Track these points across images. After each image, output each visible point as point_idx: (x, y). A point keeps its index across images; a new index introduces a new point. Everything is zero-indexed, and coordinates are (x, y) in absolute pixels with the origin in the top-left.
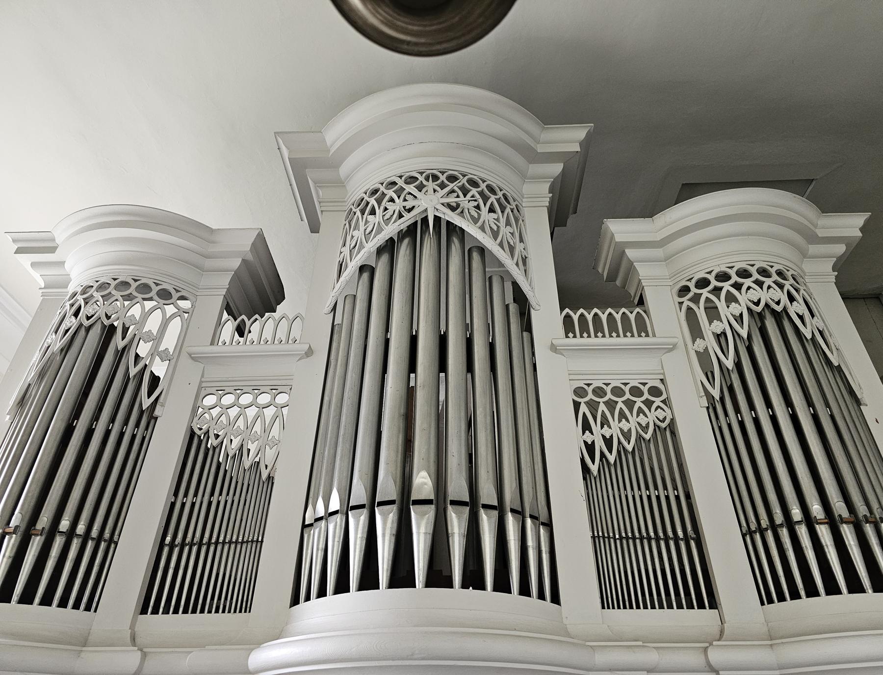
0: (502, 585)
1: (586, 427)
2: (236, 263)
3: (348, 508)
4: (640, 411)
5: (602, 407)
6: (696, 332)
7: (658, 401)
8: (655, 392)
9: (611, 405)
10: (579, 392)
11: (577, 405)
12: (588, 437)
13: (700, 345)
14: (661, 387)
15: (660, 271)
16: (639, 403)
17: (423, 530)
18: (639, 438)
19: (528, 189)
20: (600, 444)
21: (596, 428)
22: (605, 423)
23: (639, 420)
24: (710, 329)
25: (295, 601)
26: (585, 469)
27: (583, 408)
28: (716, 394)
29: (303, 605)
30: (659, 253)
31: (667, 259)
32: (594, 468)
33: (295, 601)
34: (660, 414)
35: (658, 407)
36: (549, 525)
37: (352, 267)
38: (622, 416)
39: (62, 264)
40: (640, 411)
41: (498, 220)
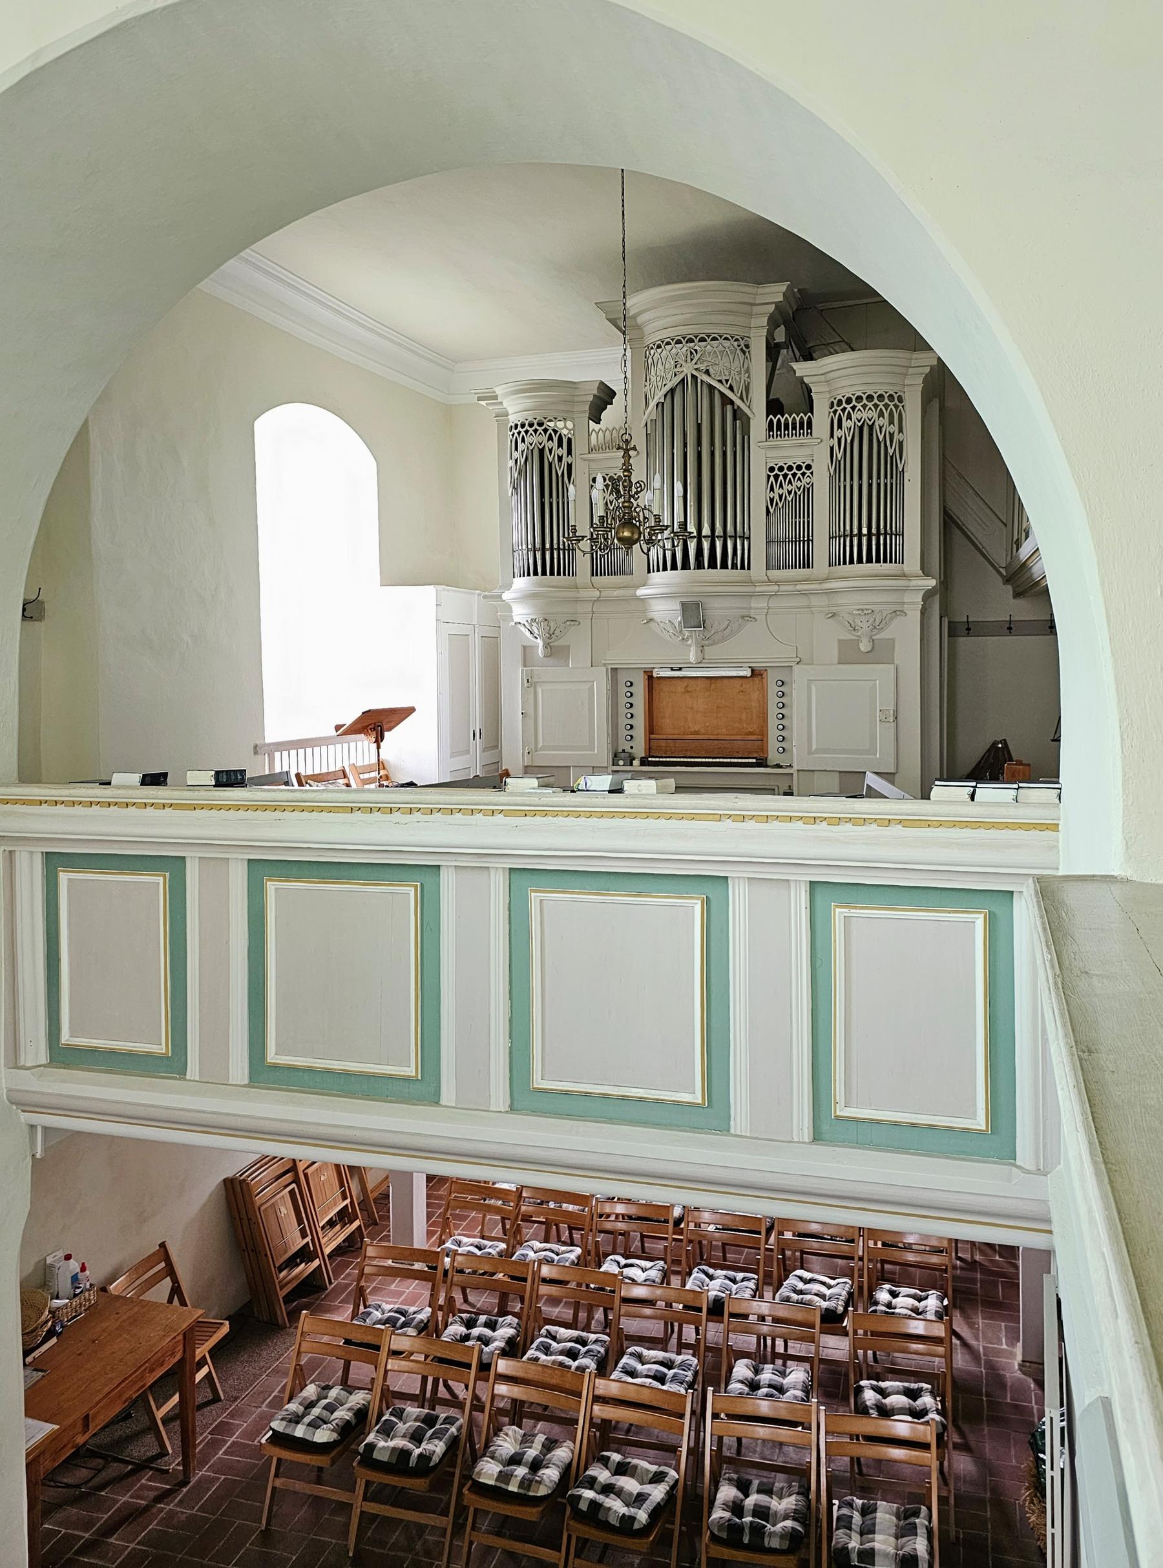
2: (591, 398)
4: (799, 479)
5: (781, 478)
6: (832, 436)
7: (808, 473)
8: (809, 467)
9: (785, 476)
11: (769, 477)
12: (772, 495)
14: (811, 464)
18: (795, 493)
20: (777, 498)
22: (781, 486)
24: (838, 433)
25: (649, 572)
26: (768, 512)
27: (772, 479)
29: (652, 574)
30: (823, 378)
32: (772, 510)
33: (649, 572)
34: (808, 480)
35: (808, 476)
36: (749, 538)
37: (652, 404)
38: (790, 482)
40: (799, 479)
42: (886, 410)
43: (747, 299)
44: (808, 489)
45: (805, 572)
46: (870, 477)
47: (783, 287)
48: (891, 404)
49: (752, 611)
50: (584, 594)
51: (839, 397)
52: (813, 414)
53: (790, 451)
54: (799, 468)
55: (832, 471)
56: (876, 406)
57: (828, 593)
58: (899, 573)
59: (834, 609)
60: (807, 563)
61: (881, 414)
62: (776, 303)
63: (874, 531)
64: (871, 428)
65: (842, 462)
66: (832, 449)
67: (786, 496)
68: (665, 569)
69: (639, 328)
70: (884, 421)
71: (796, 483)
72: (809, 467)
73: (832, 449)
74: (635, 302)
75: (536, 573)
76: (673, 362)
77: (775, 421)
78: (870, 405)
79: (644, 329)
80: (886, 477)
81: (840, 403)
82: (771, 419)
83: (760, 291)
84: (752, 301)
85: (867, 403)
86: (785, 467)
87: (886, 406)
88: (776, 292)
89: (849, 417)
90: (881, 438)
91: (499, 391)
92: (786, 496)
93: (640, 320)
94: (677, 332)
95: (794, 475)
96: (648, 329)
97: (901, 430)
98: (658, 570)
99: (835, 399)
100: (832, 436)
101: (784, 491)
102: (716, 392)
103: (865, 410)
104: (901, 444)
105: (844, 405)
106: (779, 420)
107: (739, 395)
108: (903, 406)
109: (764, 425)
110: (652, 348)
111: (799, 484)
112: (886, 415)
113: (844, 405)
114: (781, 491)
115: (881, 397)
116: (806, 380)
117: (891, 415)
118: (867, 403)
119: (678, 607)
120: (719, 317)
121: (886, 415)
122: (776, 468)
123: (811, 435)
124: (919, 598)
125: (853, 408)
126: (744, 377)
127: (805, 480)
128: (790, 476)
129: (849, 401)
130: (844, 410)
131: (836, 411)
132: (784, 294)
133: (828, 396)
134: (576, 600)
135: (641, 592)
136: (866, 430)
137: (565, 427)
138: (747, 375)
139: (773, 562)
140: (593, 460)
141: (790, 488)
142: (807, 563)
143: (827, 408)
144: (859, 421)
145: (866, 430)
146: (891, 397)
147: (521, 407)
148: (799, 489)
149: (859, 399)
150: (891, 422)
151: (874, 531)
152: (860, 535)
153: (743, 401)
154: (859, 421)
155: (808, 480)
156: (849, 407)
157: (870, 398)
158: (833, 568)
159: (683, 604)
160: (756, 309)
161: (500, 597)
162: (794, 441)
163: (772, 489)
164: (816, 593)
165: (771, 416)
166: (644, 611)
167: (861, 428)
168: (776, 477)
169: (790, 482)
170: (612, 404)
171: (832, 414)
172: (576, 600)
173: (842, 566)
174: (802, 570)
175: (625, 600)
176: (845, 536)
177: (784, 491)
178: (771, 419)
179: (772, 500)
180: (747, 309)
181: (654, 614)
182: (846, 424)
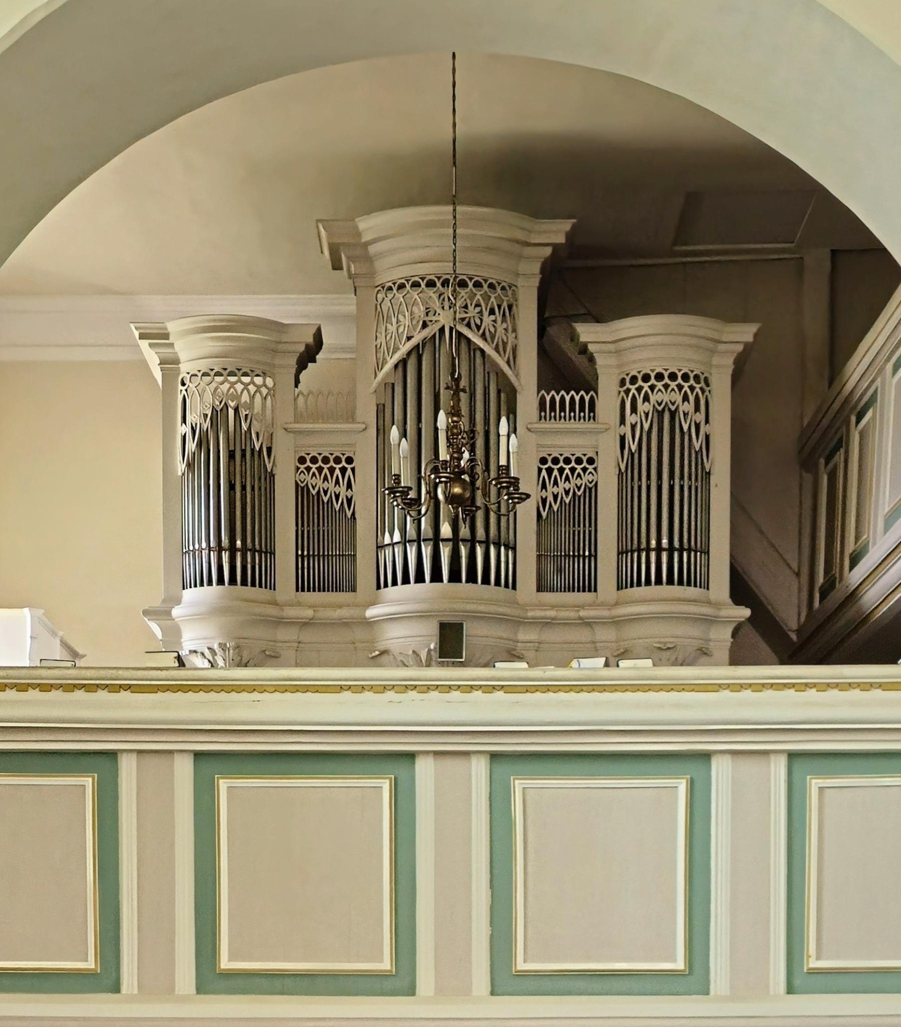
0: (486, 581)
1: (544, 486)
3: (404, 542)
4: (579, 475)
5: (556, 473)
6: (623, 421)
7: (590, 468)
8: (591, 461)
9: (561, 470)
10: (543, 461)
11: (540, 470)
12: (544, 494)
14: (595, 458)
15: (612, 361)
16: (579, 468)
17: (446, 554)
18: (574, 493)
20: (550, 499)
22: (556, 483)
23: (576, 482)
27: (544, 473)
28: (623, 469)
30: (612, 347)
31: (617, 352)
32: (544, 514)
33: (379, 587)
34: (590, 478)
36: (514, 549)
38: (567, 478)
39: (171, 345)
40: (579, 475)
41: (495, 321)
42: (692, 394)
44: (590, 489)
45: (586, 597)
47: (566, 225)
48: (698, 386)
49: (519, 644)
50: (291, 612)
51: (634, 373)
52: (597, 394)
54: (579, 461)
55: (623, 469)
56: (680, 387)
57: (617, 622)
59: (624, 645)
60: (590, 586)
61: (685, 398)
63: (676, 544)
64: (673, 414)
65: (636, 456)
66: (623, 439)
67: (562, 498)
68: (406, 581)
69: (369, 259)
70: (689, 407)
71: (574, 481)
72: (591, 461)
73: (623, 439)
75: (221, 581)
76: (422, 308)
77: (548, 398)
78: (673, 385)
81: (634, 380)
82: (543, 395)
85: (669, 382)
86: (561, 459)
87: (692, 388)
89: (646, 399)
91: (172, 327)
92: (562, 498)
93: (372, 249)
94: (428, 270)
96: (379, 265)
97: (707, 421)
98: (395, 583)
99: (627, 375)
100: (623, 421)
101: (560, 490)
102: (478, 354)
103: (666, 391)
104: (707, 437)
105: (640, 383)
107: (506, 359)
108: (709, 391)
111: (579, 482)
112: (692, 398)
114: (555, 490)
115: (686, 377)
116: (591, 348)
117: (697, 399)
118: (669, 382)
121: (692, 398)
122: (550, 459)
123: (594, 420)
125: (652, 388)
126: (511, 336)
127: (587, 478)
128: (567, 471)
129: (646, 378)
130: (639, 389)
133: (617, 371)
135: (370, 612)
137: (265, 385)
138: (514, 335)
140: (300, 432)
141: (567, 486)
142: (590, 586)
143: (615, 386)
144: (660, 404)
146: (697, 378)
147: (195, 354)
148: (579, 488)
149: (660, 377)
153: (511, 368)
154: (660, 404)
155: (590, 478)
156: (646, 386)
157: (673, 376)
158: (621, 592)
161: (168, 613)
162: (573, 425)
163: (544, 486)
165: (543, 392)
166: (373, 641)
167: (661, 414)
168: (550, 471)
169: (567, 478)
170: (314, 361)
171: (622, 394)
173: (635, 589)
174: (581, 594)
175: (345, 624)
177: (560, 490)
178: (543, 395)
179: (544, 501)
182: (642, 407)
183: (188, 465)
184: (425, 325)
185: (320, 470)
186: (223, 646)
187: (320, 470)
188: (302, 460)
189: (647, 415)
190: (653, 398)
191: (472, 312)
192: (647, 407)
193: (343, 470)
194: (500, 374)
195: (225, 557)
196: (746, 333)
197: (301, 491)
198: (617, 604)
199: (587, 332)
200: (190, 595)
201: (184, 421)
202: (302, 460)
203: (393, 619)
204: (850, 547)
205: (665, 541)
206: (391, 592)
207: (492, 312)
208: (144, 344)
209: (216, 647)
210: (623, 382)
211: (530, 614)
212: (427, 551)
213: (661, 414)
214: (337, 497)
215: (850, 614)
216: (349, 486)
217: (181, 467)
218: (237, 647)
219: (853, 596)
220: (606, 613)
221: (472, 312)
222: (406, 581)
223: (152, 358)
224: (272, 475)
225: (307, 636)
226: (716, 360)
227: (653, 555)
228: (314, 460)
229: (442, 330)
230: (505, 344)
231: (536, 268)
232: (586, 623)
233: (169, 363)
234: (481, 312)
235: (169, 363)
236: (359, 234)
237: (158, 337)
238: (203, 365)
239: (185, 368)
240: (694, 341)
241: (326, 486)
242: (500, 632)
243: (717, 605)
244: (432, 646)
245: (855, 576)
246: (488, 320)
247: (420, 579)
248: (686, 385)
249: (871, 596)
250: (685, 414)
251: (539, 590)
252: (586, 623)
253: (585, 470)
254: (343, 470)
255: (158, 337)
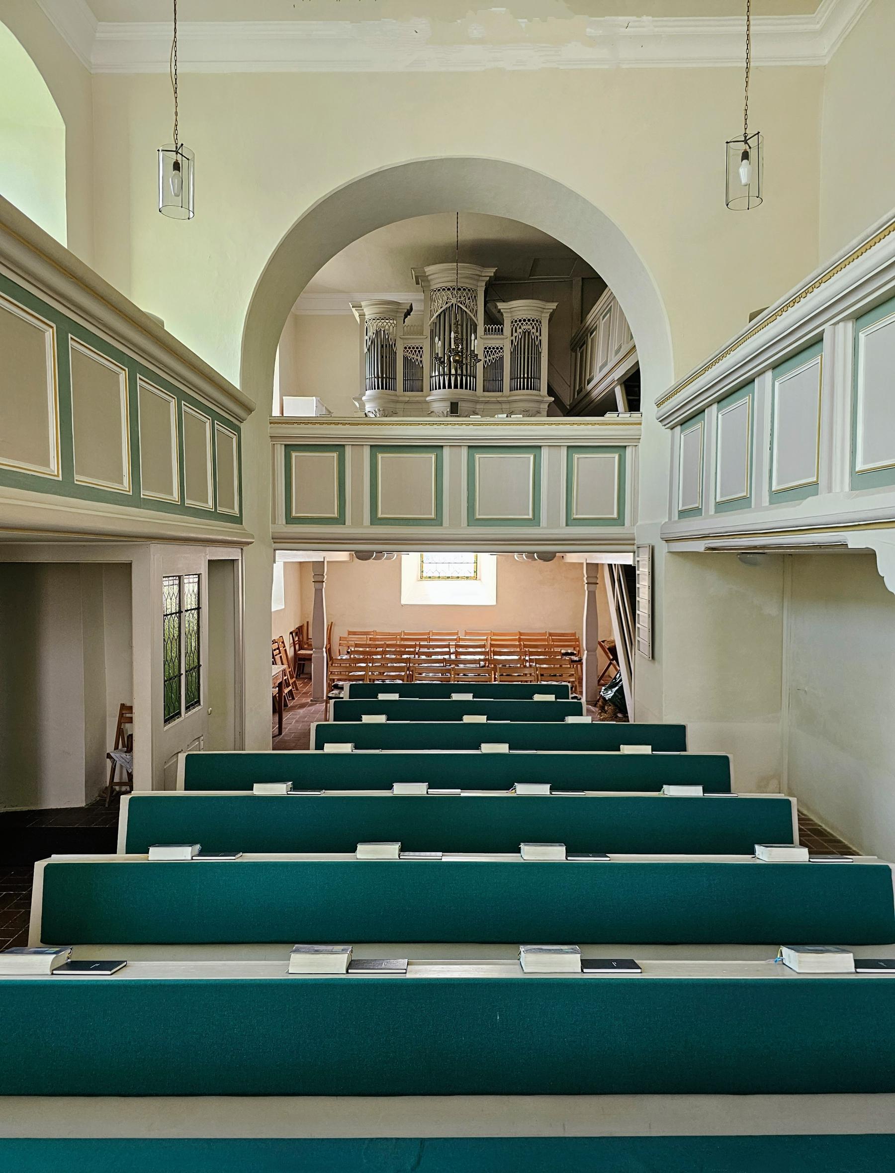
0: (466, 388)
1: (486, 357)
3: (439, 375)
6: (512, 335)
7: (501, 351)
8: (501, 348)
9: (492, 352)
10: (486, 348)
11: (484, 351)
12: (486, 359)
13: (512, 338)
15: (509, 315)
18: (496, 359)
19: (480, 284)
20: (488, 361)
21: (488, 357)
22: (490, 356)
24: (515, 334)
25: (431, 390)
26: (484, 366)
27: (486, 352)
28: (512, 351)
30: (509, 310)
32: (486, 366)
33: (431, 390)
34: (501, 354)
38: (494, 354)
39: (363, 310)
40: (497, 353)
41: (470, 302)
43: (478, 273)
45: (500, 394)
46: (528, 354)
48: (537, 324)
50: (401, 399)
53: (494, 341)
54: (497, 348)
55: (512, 351)
56: (532, 324)
57: (509, 402)
58: (539, 394)
59: (513, 409)
60: (501, 390)
61: (533, 328)
62: (490, 277)
63: (530, 376)
64: (529, 333)
66: (512, 341)
68: (440, 388)
69: (428, 281)
70: (534, 331)
72: (501, 348)
73: (512, 341)
74: (429, 270)
76: (446, 297)
78: (529, 323)
79: (431, 283)
80: (532, 354)
83: (485, 271)
84: (480, 274)
87: (535, 324)
88: (491, 272)
89: (520, 328)
90: (533, 337)
91: (363, 304)
93: (429, 278)
94: (449, 285)
95: (495, 351)
96: (432, 283)
97: (540, 335)
100: (512, 335)
104: (540, 340)
106: (495, 327)
109: (483, 329)
110: (435, 291)
112: (535, 328)
113: (518, 322)
114: (490, 358)
115: (533, 321)
116: (502, 310)
119: (449, 404)
120: (465, 279)
121: (535, 328)
124: (546, 406)
125: (522, 324)
129: (520, 321)
130: (518, 324)
131: (514, 325)
132: (494, 273)
133: (510, 318)
134: (397, 402)
136: (527, 333)
137: (393, 323)
139: (486, 389)
140: (406, 339)
142: (501, 390)
143: (510, 324)
145: (527, 333)
146: (537, 321)
147: (370, 312)
149: (524, 320)
150: (537, 331)
151: (530, 376)
152: (524, 378)
155: (501, 354)
157: (529, 320)
159: (451, 403)
160: (481, 278)
163: (486, 357)
164: (505, 402)
166: (429, 408)
168: (488, 352)
169: (494, 354)
170: (410, 315)
172: (397, 402)
176: (517, 378)
180: (476, 277)
181: (435, 410)
182: (519, 330)
183: (368, 349)
184: (447, 303)
185: (411, 351)
186: (379, 410)
187: (411, 351)
188: (406, 348)
189: (520, 333)
190: (522, 328)
191: (463, 298)
192: (520, 330)
193: (419, 351)
194: (471, 319)
195: (380, 380)
196: (554, 306)
197: (405, 358)
198: (510, 396)
199: (500, 305)
200: (368, 392)
201: (367, 335)
202: (406, 348)
203: (434, 401)
204: (588, 377)
205: (526, 375)
206: (434, 392)
207: (469, 299)
208: (354, 309)
209: (377, 410)
210: (512, 322)
211: (481, 399)
212: (447, 378)
213: (525, 333)
214: (417, 360)
215: (587, 399)
216: (421, 357)
217: (366, 350)
218: (383, 410)
219: (589, 394)
220: (506, 399)
221: (463, 298)
222: (440, 388)
223: (356, 314)
224: (396, 353)
225: (407, 406)
226: (543, 315)
227: (522, 380)
228: (409, 348)
229: (452, 305)
230: (473, 310)
231: (484, 284)
232: (499, 402)
233: (362, 316)
234: (465, 299)
235: (362, 316)
236: (425, 273)
237: (358, 306)
238: (373, 316)
239: (367, 317)
240: (536, 308)
241: (413, 356)
242: (470, 405)
243: (543, 397)
244: (448, 410)
245: (590, 387)
246: (467, 301)
247: (444, 387)
248: (533, 323)
249: (595, 394)
250: (533, 333)
251: (484, 391)
252: (499, 402)
253: (499, 351)
254: (419, 351)
255: (358, 306)
